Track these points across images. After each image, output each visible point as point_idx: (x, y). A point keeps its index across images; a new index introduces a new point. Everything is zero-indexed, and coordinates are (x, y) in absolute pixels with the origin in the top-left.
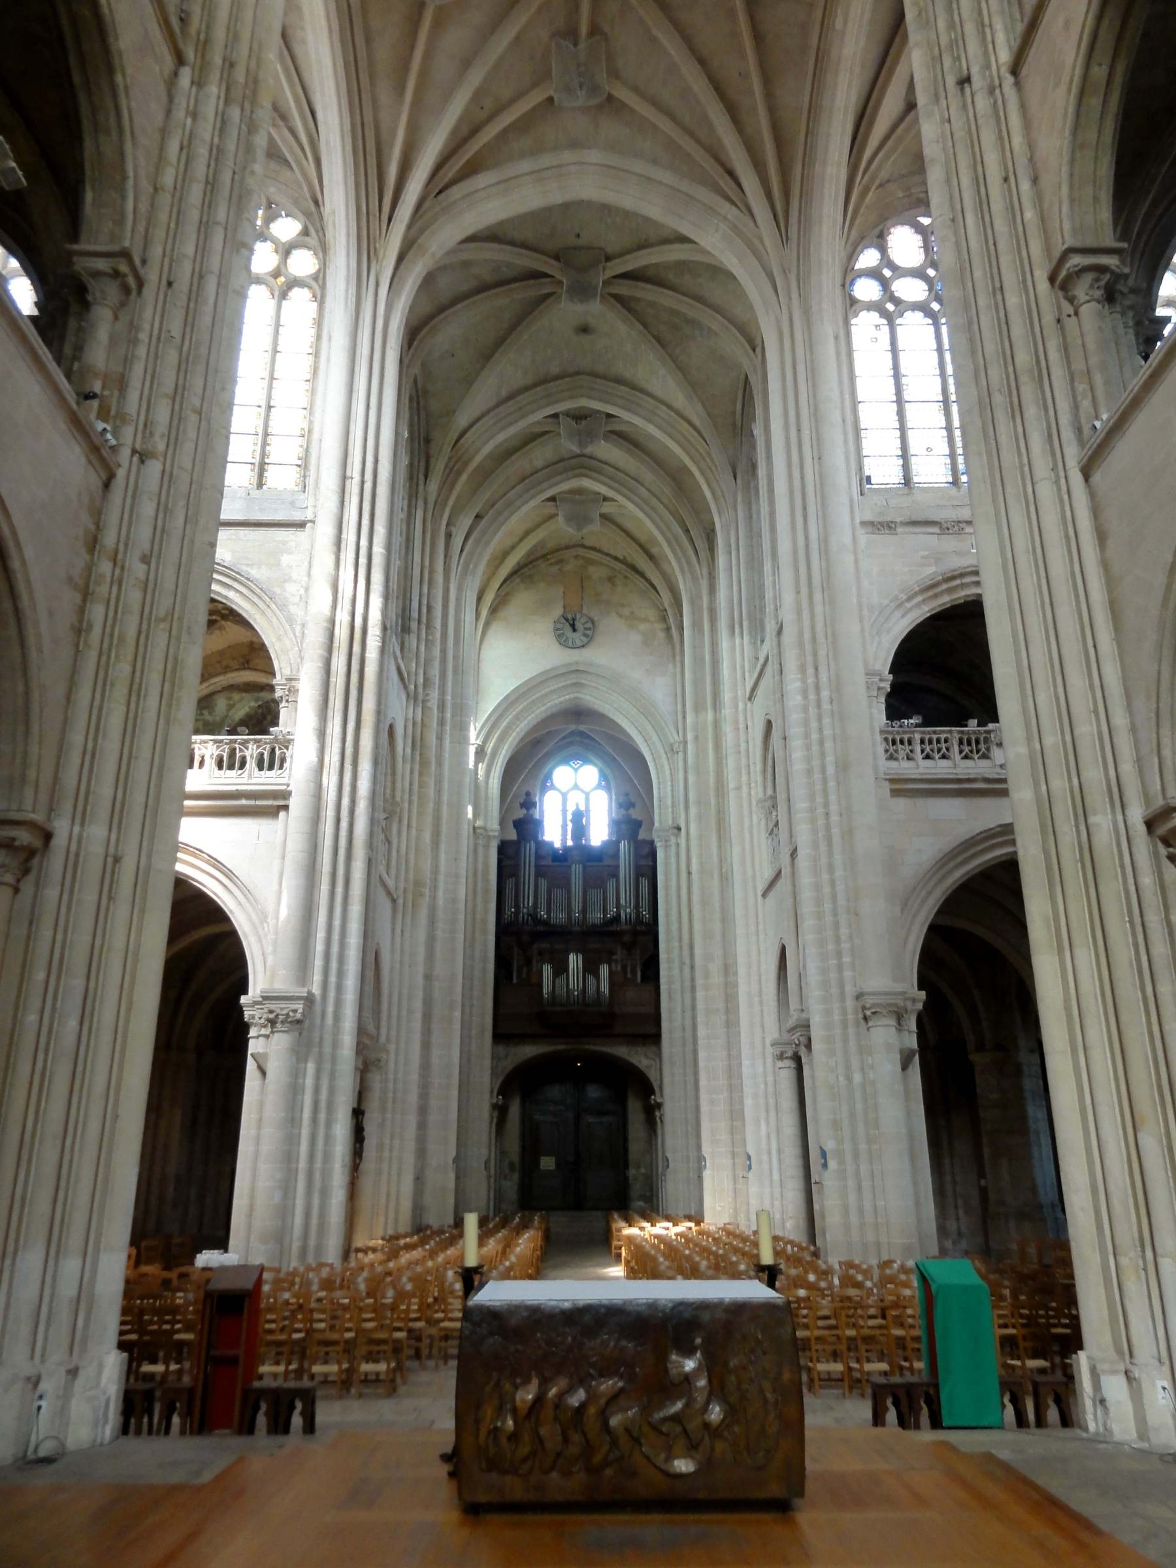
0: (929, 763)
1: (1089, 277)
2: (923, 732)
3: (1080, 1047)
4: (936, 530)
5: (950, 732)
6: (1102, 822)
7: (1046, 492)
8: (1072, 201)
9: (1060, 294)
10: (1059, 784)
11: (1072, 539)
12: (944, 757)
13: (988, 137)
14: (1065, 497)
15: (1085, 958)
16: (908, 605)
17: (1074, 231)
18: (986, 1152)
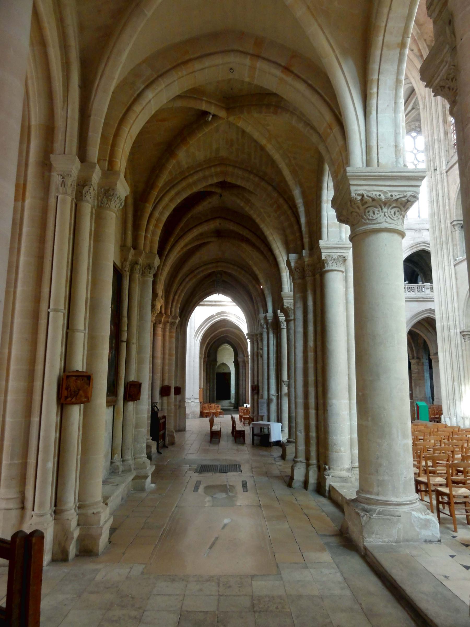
0: (409, 293)
1: (458, 225)
2: (408, 286)
3: (445, 368)
4: (414, 231)
5: (415, 285)
6: (452, 331)
7: (447, 268)
8: (456, 208)
9: (452, 227)
10: (445, 323)
11: (451, 278)
12: (413, 292)
13: (440, 186)
14: (450, 270)
15: (448, 354)
16: (406, 252)
17: (456, 216)
18: (413, 384)
